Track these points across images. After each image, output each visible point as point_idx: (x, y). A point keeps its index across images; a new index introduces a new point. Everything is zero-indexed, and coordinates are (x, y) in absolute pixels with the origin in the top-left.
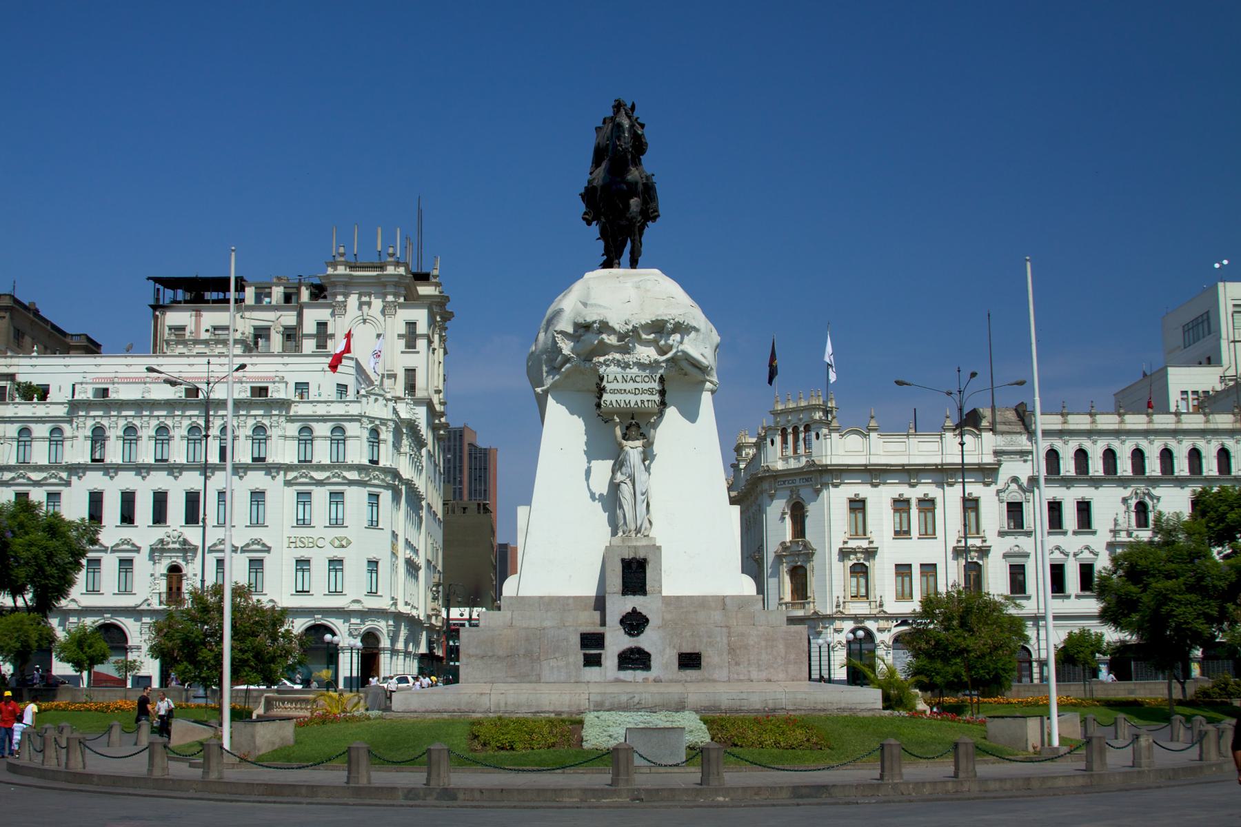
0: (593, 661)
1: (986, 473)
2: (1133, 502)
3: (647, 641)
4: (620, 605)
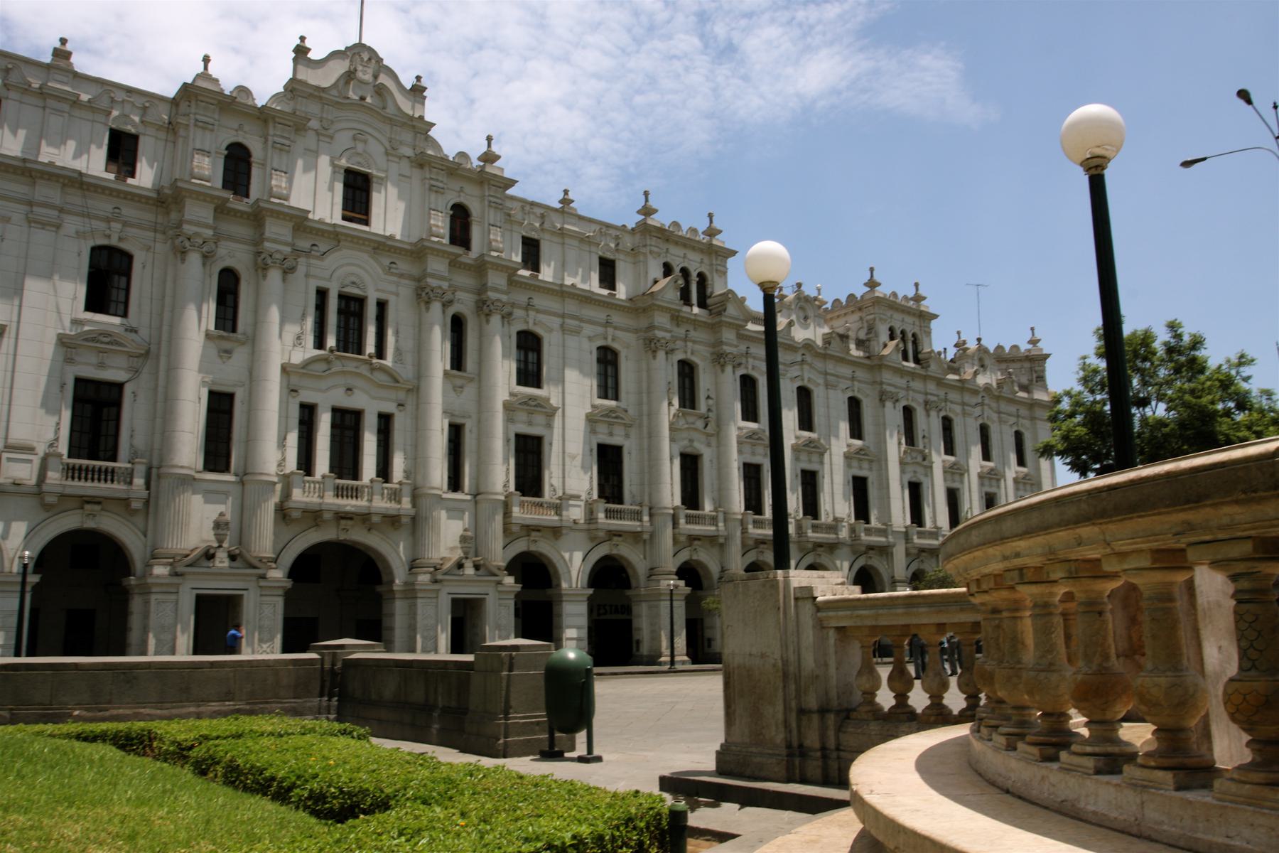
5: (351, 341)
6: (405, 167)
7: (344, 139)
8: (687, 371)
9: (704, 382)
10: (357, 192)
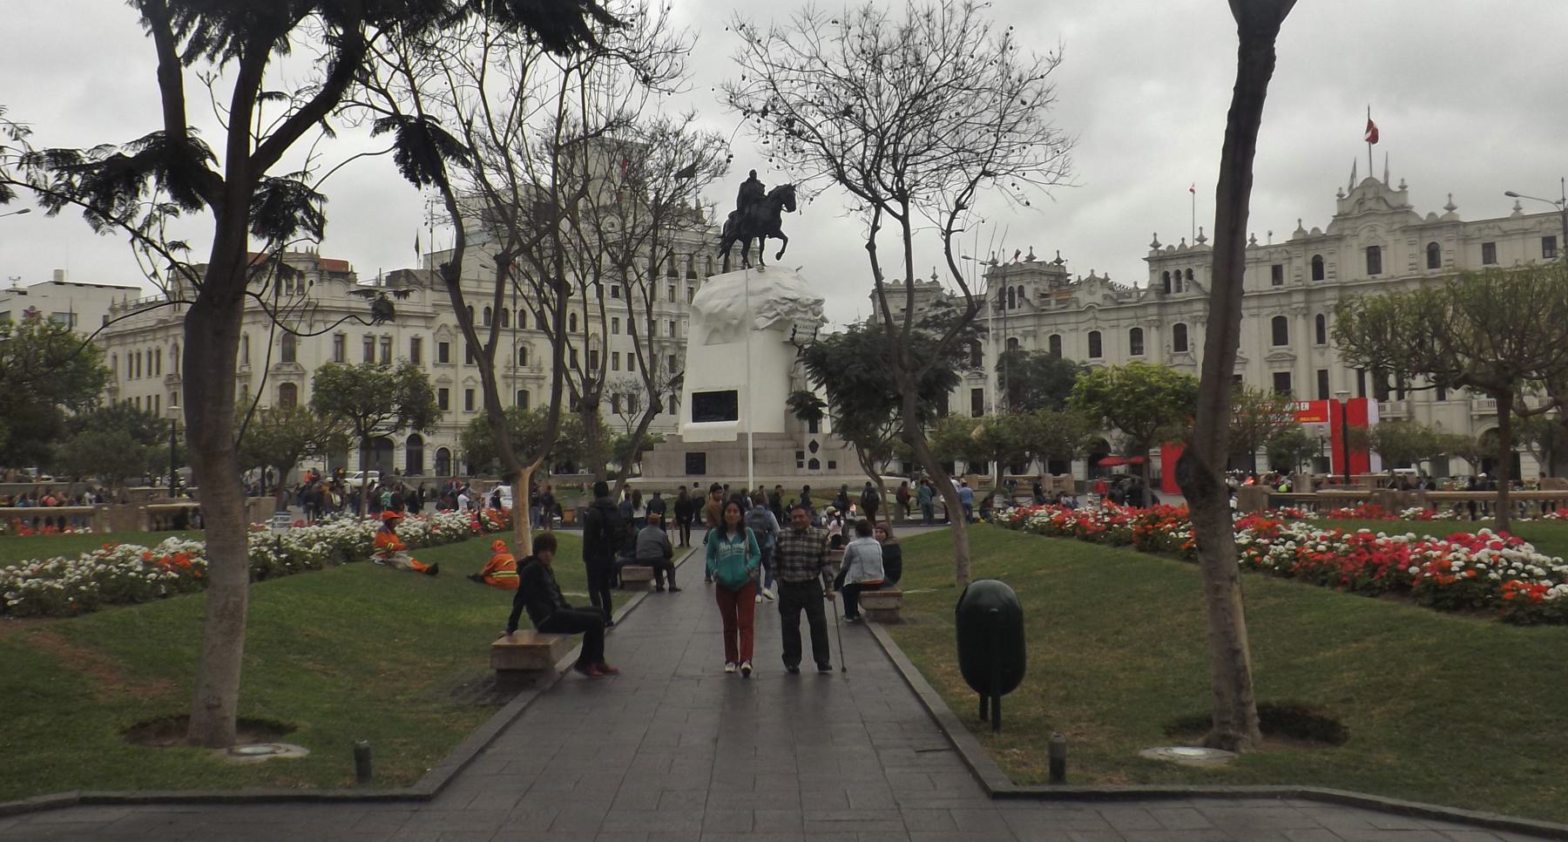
0: (800, 465)
1: (427, 318)
2: (519, 347)
3: (819, 455)
4: (809, 438)
6: (1399, 235)
7: (1364, 234)
10: (1374, 255)
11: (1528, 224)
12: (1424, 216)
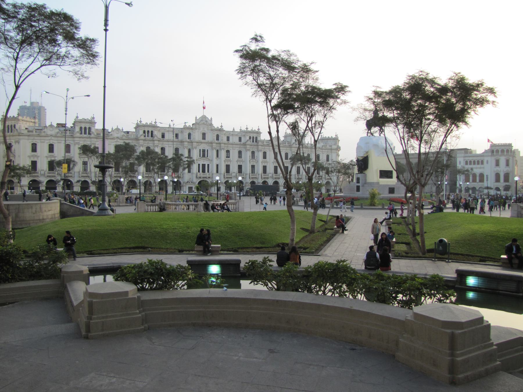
5: (204, 156)
7: (202, 129)
8: (253, 153)
9: (256, 154)
11: (236, 133)
12: (216, 127)
